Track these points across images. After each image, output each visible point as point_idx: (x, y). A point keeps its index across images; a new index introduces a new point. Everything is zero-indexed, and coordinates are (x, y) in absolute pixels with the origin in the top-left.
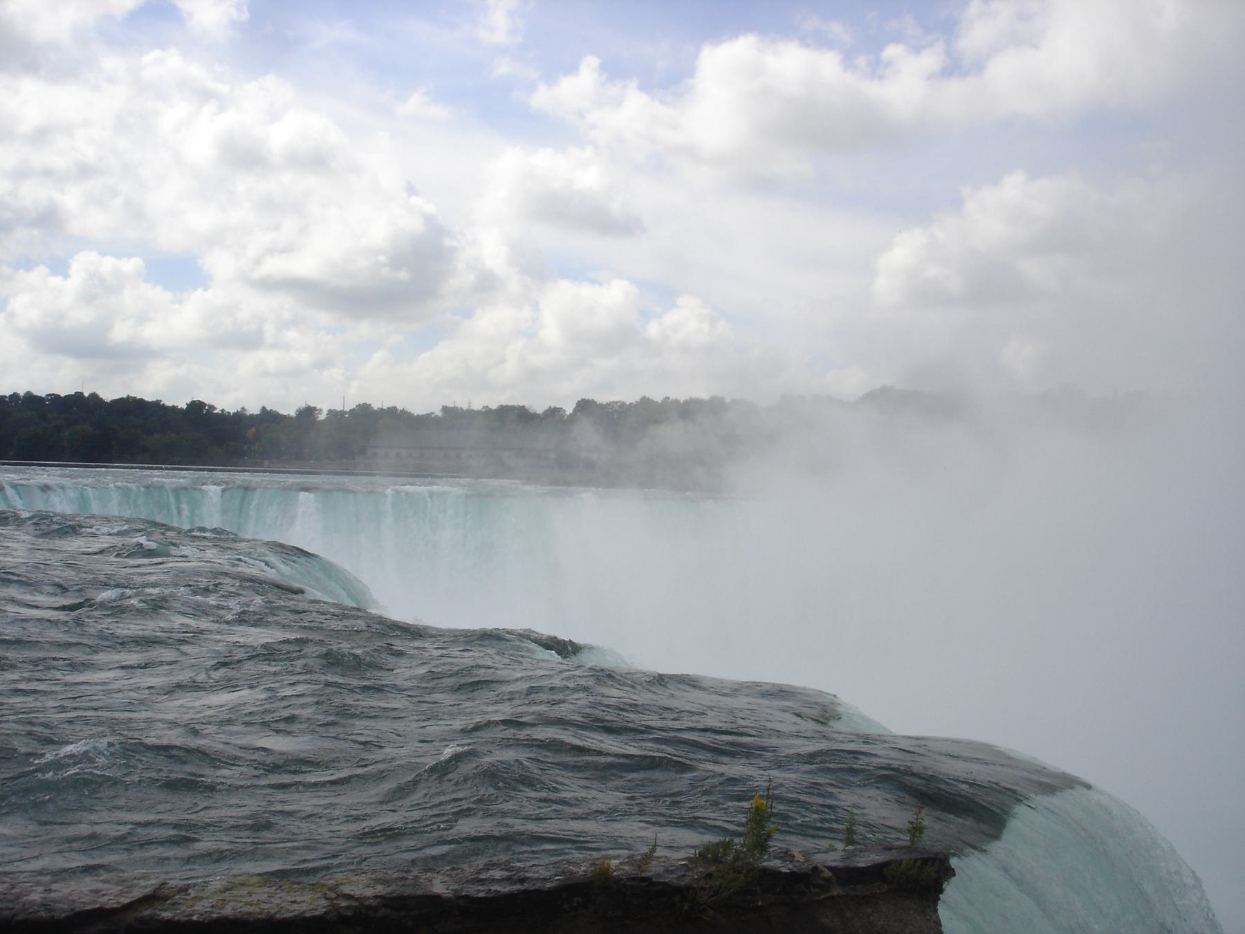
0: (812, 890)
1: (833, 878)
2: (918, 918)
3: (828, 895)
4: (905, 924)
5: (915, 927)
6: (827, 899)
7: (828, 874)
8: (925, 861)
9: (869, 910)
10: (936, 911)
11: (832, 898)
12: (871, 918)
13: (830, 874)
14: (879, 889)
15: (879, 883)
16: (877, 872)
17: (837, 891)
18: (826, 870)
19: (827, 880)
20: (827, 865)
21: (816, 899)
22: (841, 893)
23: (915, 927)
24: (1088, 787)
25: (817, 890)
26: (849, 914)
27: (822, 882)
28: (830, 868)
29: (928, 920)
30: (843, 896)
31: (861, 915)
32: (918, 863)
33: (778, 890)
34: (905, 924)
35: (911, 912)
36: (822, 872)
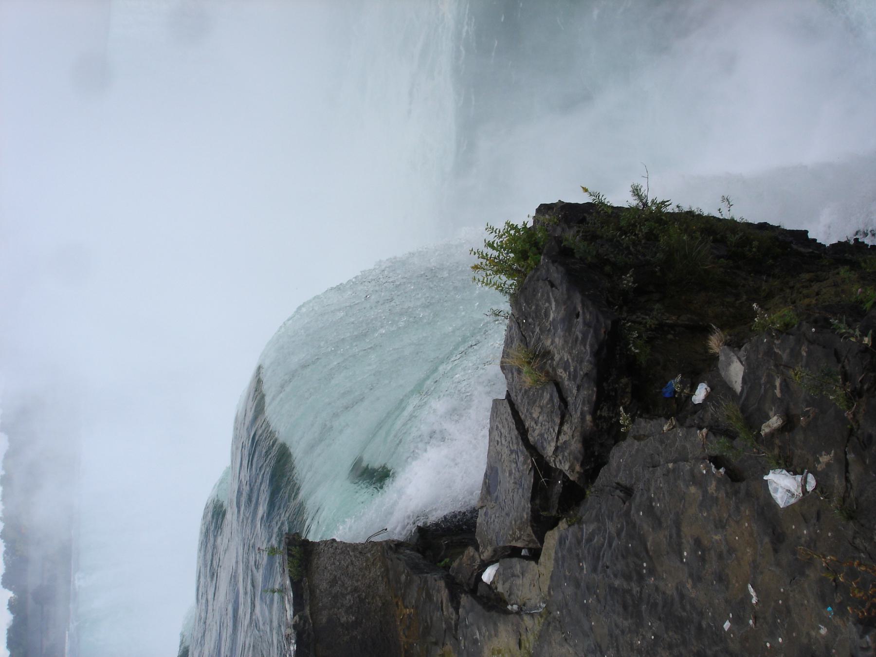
0: (306, 628)
1: (299, 614)
2: (322, 559)
3: (310, 618)
4: (325, 568)
5: (327, 563)
6: (311, 617)
7: (297, 617)
8: (289, 555)
9: (318, 591)
10: (318, 544)
11: (311, 614)
12: (322, 590)
13: (297, 616)
14: (306, 583)
15: (302, 583)
16: (296, 585)
17: (307, 611)
18: (295, 618)
19: (300, 619)
20: (292, 617)
21: (312, 625)
22: (308, 608)
23: (327, 563)
24: (259, 368)
25: (307, 625)
26: (320, 604)
27: (302, 622)
28: (294, 615)
29: (324, 551)
30: (310, 607)
31: (321, 597)
32: (291, 559)
33: (307, 651)
34: (325, 568)
35: (319, 562)
36: (296, 621)
